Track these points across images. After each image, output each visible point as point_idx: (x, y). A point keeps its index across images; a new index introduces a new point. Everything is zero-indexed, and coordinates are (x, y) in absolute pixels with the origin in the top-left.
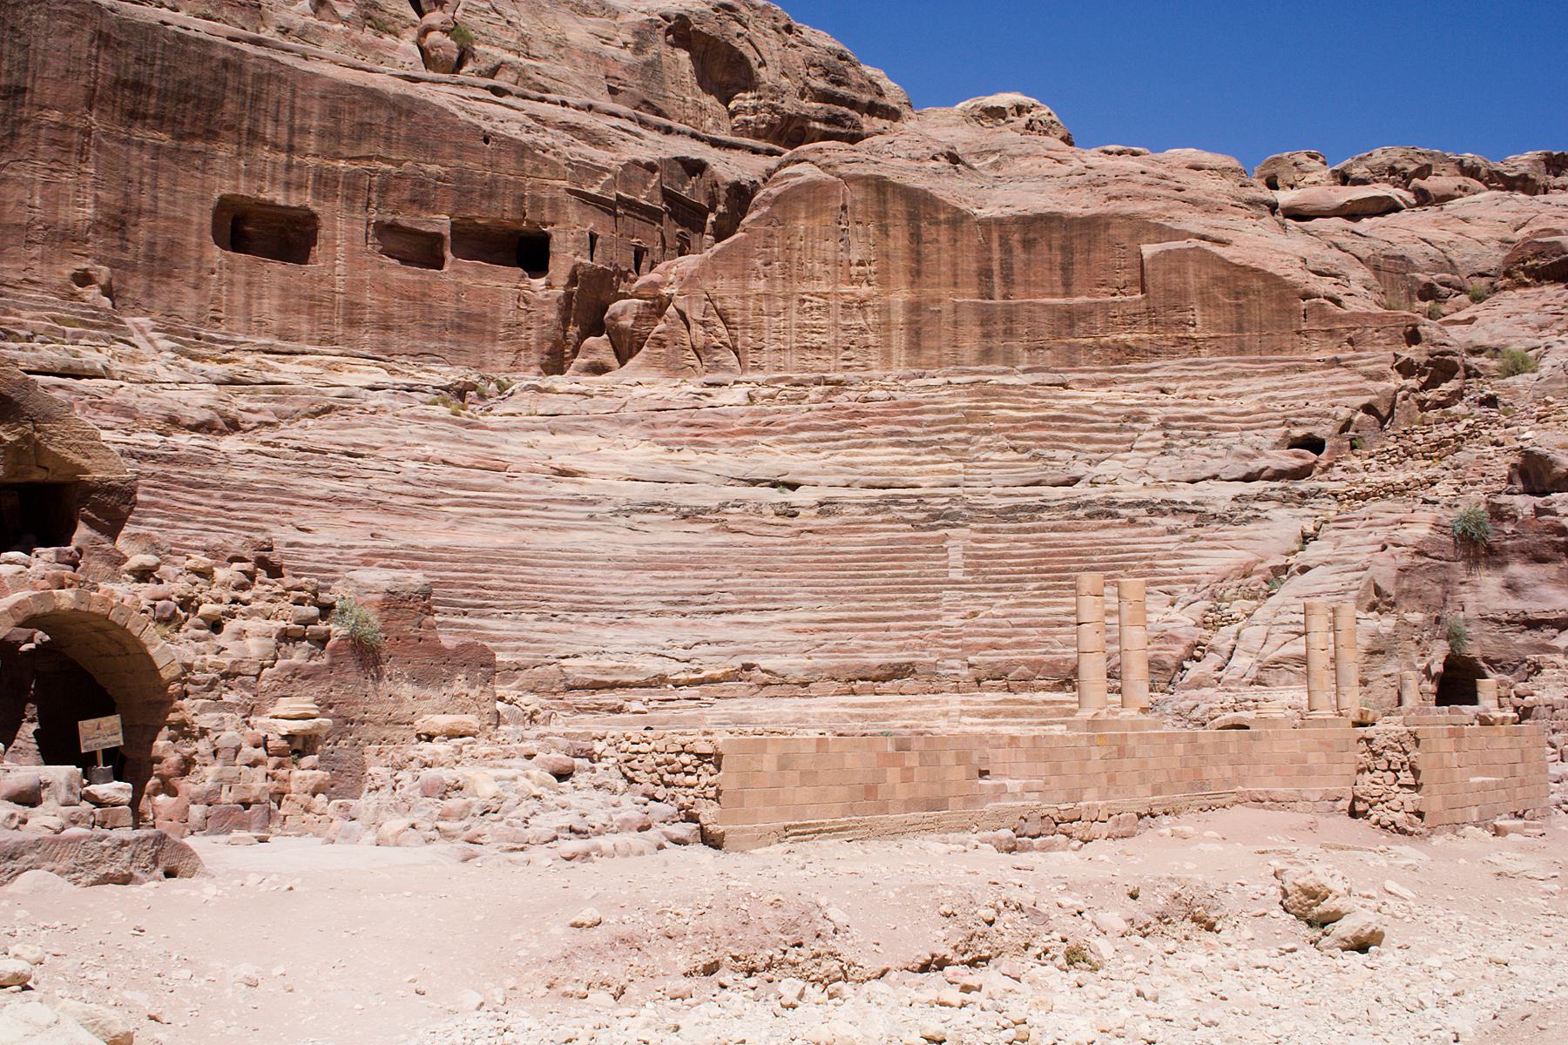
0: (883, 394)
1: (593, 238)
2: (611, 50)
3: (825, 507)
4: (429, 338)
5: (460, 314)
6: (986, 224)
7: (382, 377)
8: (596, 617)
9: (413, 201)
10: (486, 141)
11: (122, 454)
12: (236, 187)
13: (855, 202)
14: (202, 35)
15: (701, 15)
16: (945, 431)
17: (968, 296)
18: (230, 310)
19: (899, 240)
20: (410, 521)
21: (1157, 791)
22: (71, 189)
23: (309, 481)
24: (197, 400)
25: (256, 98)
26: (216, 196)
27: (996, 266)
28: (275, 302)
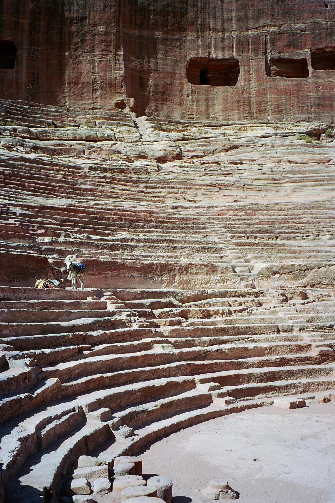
4: (302, 113)
5: (319, 98)
7: (270, 131)
9: (289, 45)
10: (326, 6)
11: (91, 168)
12: (198, 53)
18: (198, 113)
20: (263, 193)
22: (113, 63)
25: (204, 7)
26: (188, 59)
28: (221, 107)
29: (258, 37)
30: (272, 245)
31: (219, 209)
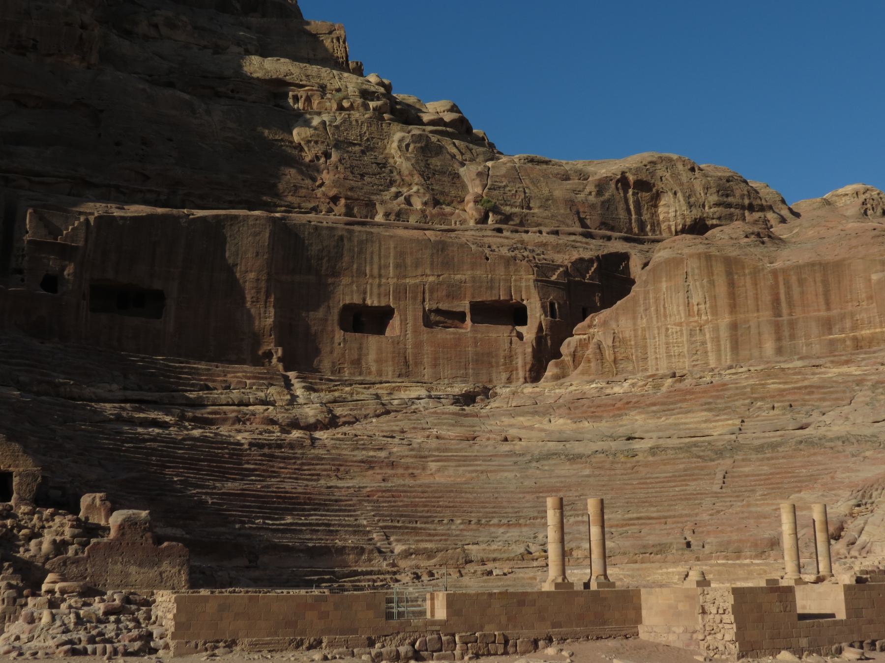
0: (708, 379)
1: (552, 305)
2: (581, 197)
3: (653, 451)
6: (775, 273)
8: (495, 521)
10: (487, 259)
13: (693, 269)
14: (330, 224)
15: (638, 170)
16: (737, 400)
17: (766, 314)
19: (722, 289)
21: (554, 626)
22: (262, 310)
23: (355, 453)
24: (311, 413)
25: (360, 252)
27: (782, 297)
29: (416, 286)
30: (413, 528)
31: (368, 489)
